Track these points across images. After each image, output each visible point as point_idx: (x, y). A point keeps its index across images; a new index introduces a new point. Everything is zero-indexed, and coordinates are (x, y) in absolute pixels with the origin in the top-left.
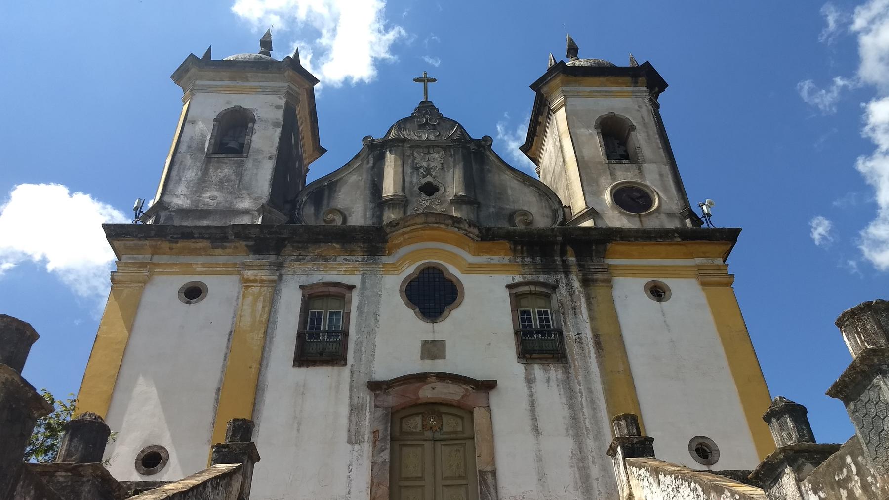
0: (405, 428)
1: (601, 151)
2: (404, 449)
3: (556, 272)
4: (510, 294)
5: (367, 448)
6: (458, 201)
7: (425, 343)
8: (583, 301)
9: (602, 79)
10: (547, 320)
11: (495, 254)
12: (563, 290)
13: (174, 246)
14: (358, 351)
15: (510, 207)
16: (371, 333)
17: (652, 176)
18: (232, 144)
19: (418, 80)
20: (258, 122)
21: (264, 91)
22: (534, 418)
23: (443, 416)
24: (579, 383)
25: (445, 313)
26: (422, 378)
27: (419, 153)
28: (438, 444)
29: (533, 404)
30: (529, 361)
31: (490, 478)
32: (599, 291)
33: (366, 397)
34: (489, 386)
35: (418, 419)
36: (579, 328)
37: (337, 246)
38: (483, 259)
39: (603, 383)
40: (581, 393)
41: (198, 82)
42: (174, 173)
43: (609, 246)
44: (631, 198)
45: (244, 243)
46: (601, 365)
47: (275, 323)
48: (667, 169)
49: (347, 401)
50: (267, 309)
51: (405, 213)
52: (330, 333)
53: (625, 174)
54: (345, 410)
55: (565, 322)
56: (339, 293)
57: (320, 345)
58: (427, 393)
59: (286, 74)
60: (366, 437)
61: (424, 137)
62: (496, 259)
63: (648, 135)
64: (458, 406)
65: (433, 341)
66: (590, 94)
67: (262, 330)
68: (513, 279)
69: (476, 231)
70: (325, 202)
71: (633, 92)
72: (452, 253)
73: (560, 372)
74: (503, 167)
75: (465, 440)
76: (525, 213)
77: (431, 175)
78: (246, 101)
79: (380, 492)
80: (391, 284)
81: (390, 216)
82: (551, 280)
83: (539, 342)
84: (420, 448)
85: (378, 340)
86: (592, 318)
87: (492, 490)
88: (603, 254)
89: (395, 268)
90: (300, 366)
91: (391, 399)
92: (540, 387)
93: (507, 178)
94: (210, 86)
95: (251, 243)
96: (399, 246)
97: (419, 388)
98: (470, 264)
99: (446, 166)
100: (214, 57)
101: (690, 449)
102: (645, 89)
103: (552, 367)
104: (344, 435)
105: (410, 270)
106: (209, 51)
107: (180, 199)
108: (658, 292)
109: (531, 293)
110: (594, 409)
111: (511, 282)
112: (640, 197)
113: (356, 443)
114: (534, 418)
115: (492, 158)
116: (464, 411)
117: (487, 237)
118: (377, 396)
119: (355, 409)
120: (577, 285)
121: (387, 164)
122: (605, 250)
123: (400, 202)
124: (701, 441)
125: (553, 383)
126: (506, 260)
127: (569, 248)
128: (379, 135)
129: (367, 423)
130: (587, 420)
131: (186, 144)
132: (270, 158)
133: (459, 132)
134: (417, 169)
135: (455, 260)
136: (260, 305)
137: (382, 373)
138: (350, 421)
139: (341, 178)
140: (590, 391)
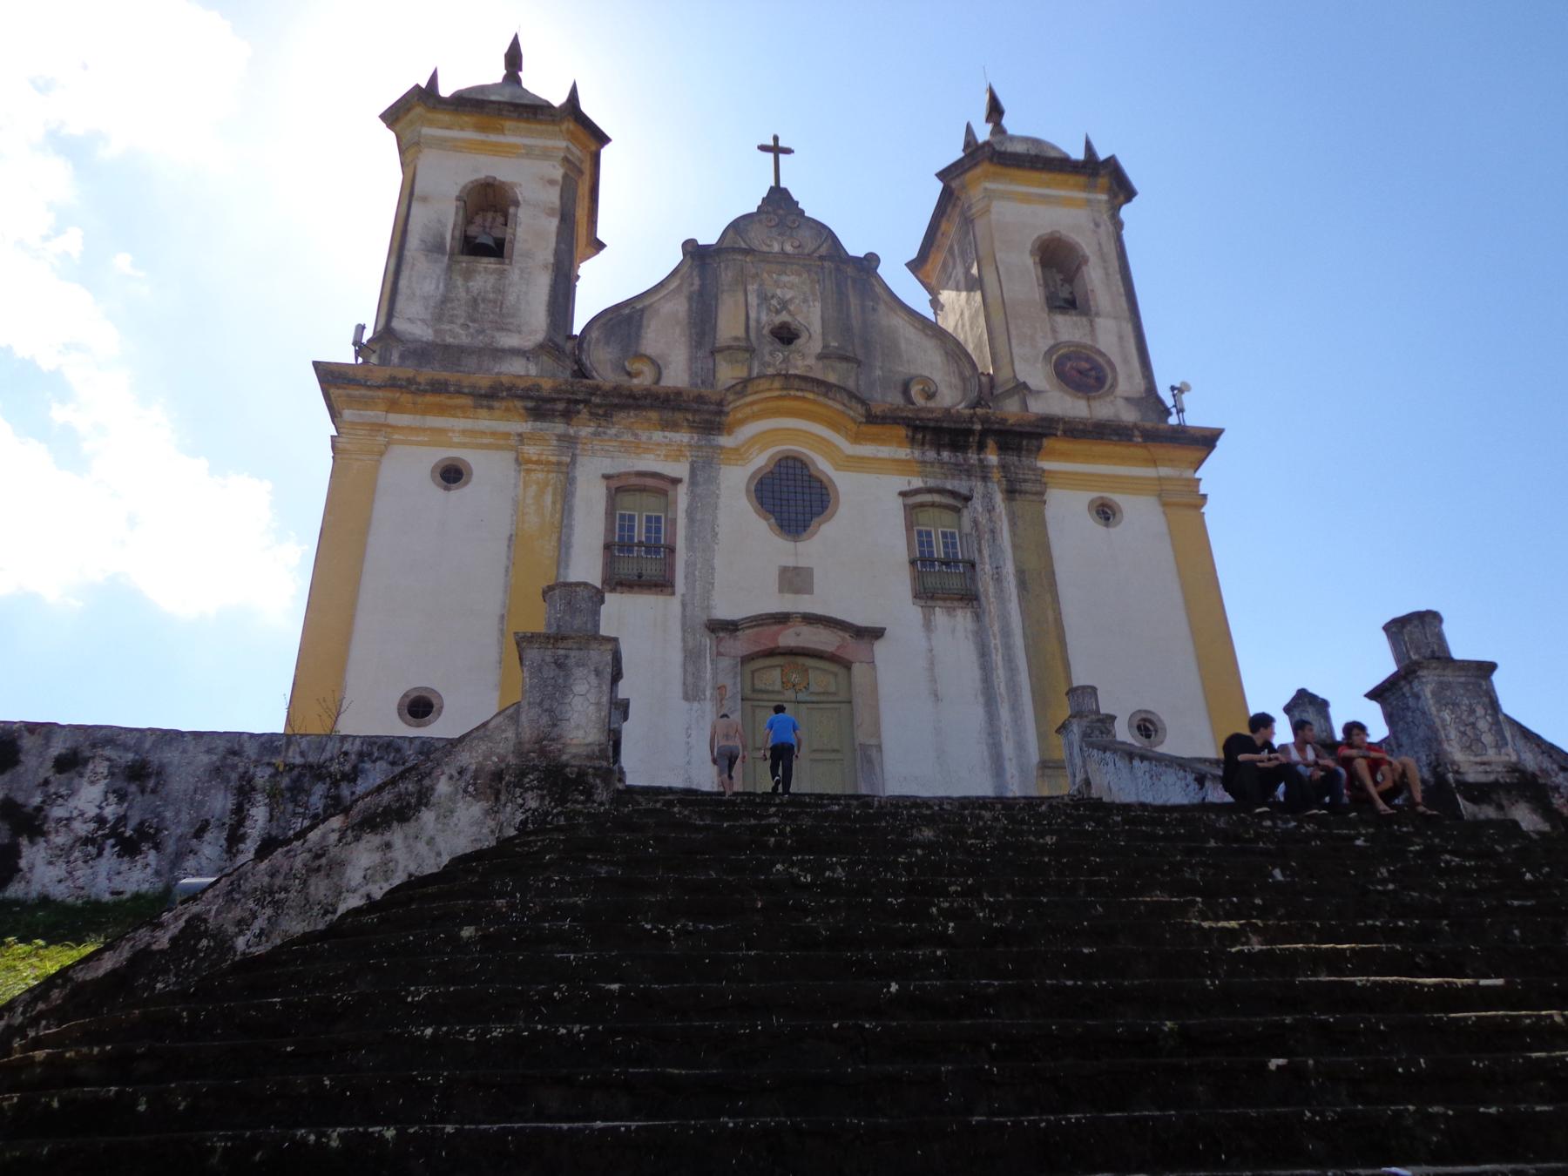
0: (759, 685)
1: (1037, 294)
7: (784, 571)
9: (1045, 176)
12: (977, 504)
13: (419, 400)
15: (904, 370)
17: (1107, 337)
19: (763, 148)
21: (529, 153)
22: (933, 680)
26: (782, 619)
27: (770, 273)
30: (930, 603)
31: (874, 753)
34: (877, 633)
35: (777, 673)
37: (654, 415)
38: (867, 450)
39: (1025, 636)
41: (426, 131)
42: (403, 283)
43: (1046, 442)
45: (519, 404)
46: (1025, 614)
48: (1128, 328)
49: (678, 644)
50: (558, 506)
53: (1069, 329)
54: (676, 657)
55: (980, 551)
56: (661, 486)
58: (788, 638)
59: (564, 127)
60: (708, 694)
61: (776, 248)
62: (885, 451)
63: (1107, 274)
64: (832, 658)
65: (795, 568)
66: (1027, 199)
67: (555, 537)
72: (824, 439)
76: (925, 380)
77: (789, 312)
78: (503, 170)
80: (734, 480)
82: (961, 485)
83: (944, 578)
85: (717, 562)
86: (1015, 547)
89: (738, 454)
91: (740, 645)
93: (898, 322)
94: (445, 140)
95: (530, 404)
96: (742, 422)
100: (445, 90)
102: (1104, 197)
104: (677, 689)
105: (760, 460)
106: (434, 79)
107: (415, 325)
108: (1105, 513)
109: (933, 505)
111: (906, 488)
115: (878, 289)
118: (719, 640)
119: (691, 656)
120: (999, 498)
122: (1039, 448)
123: (745, 349)
127: (991, 443)
129: (708, 676)
136: (548, 499)
137: (725, 610)
138: (685, 671)
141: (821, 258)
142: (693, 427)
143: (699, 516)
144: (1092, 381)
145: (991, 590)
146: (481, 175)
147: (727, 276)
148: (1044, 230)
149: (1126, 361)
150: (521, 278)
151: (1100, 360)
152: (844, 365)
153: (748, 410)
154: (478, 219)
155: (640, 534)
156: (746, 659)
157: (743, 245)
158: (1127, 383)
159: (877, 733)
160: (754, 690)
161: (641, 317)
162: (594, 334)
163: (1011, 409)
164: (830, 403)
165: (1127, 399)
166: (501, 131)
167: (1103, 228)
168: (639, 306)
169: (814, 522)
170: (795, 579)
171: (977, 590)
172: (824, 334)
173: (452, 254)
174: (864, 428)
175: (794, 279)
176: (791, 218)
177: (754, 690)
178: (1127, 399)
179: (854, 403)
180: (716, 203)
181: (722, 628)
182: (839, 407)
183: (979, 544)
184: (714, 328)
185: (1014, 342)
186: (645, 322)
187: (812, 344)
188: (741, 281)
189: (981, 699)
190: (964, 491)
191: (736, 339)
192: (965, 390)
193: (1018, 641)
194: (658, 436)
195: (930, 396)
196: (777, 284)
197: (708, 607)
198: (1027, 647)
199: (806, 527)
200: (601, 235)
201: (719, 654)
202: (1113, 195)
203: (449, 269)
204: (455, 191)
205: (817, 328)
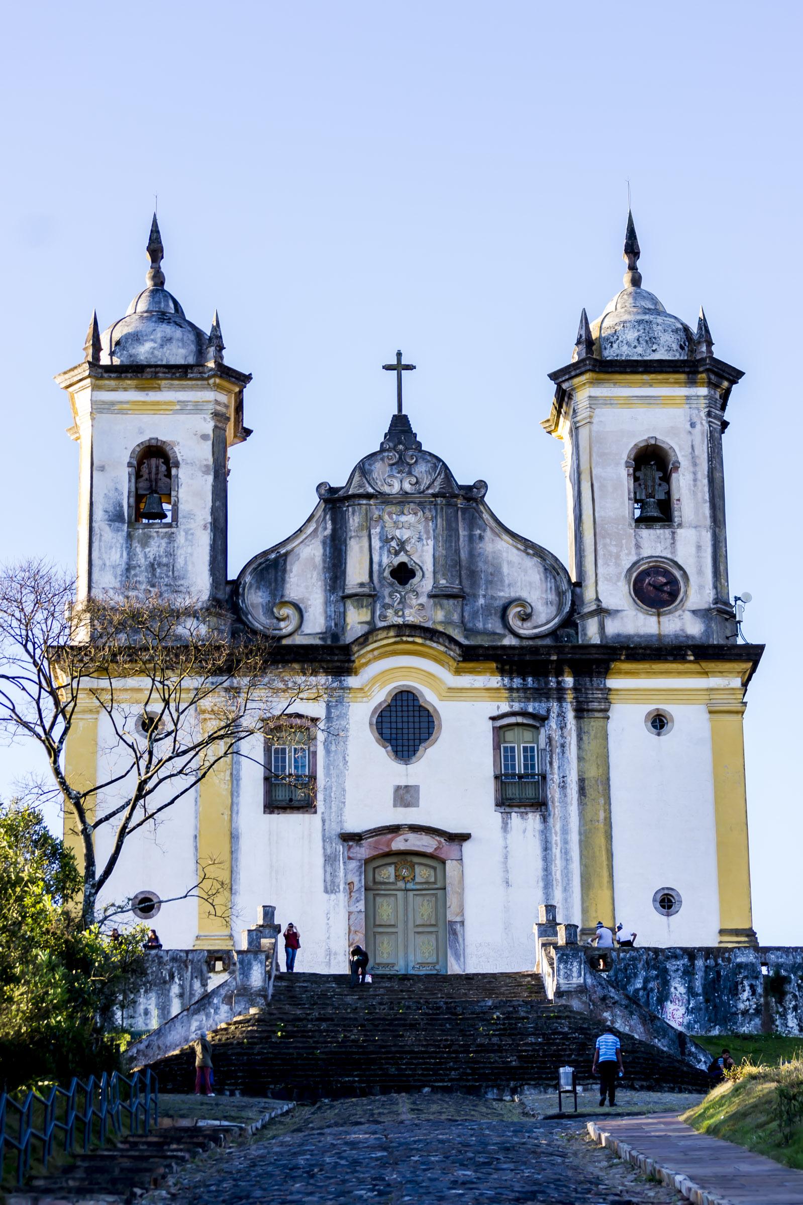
2: (379, 900)
3: (548, 699)
4: (494, 728)
5: (342, 897)
7: (398, 788)
10: (532, 757)
11: (479, 673)
12: (553, 723)
15: (505, 594)
16: (341, 775)
17: (687, 546)
19: (388, 368)
21: (183, 408)
23: (416, 866)
24: (556, 833)
25: (418, 754)
26: (395, 829)
27: (390, 514)
28: (411, 894)
30: (508, 810)
31: (458, 927)
32: (592, 725)
34: (462, 838)
35: (391, 870)
36: (565, 771)
37: (296, 666)
38: (466, 681)
39: (580, 834)
44: (657, 587)
46: (582, 814)
48: (707, 537)
49: (321, 851)
51: (373, 613)
53: (654, 543)
54: (320, 860)
55: (551, 763)
56: (304, 726)
58: (399, 844)
59: (211, 381)
60: (341, 888)
61: (396, 489)
63: (695, 480)
65: (406, 787)
66: (628, 402)
67: (228, 773)
68: (498, 707)
71: (688, 398)
74: (498, 529)
75: (438, 890)
80: (360, 714)
83: (520, 790)
84: (393, 899)
85: (348, 785)
86: (580, 759)
88: (605, 672)
90: (271, 812)
91: (363, 851)
94: (113, 403)
97: (392, 840)
98: (450, 689)
99: (424, 537)
101: (654, 900)
103: (530, 815)
104: (320, 886)
105: (380, 696)
108: (659, 722)
109: (518, 724)
111: (495, 713)
113: (332, 892)
115: (486, 516)
116: (436, 860)
117: (471, 656)
119: (330, 860)
120: (570, 715)
123: (368, 597)
124: (666, 892)
125: (530, 833)
127: (567, 669)
128: (339, 480)
131: (101, 507)
133: (442, 476)
138: (325, 871)
139: (292, 550)
140: (566, 842)
141: (435, 496)
142: (327, 672)
143: (333, 748)
144: (665, 596)
145: (557, 796)
146: (145, 438)
147: (354, 521)
149: (700, 572)
150: (186, 539)
151: (677, 574)
152: (451, 602)
153: (370, 656)
156: (367, 861)
157: (371, 490)
158: (698, 593)
159: (462, 912)
161: (285, 561)
162: (248, 579)
163: (592, 632)
164: (435, 645)
166: (159, 389)
167: (698, 426)
168: (283, 551)
169: (421, 748)
170: (405, 796)
172: (435, 573)
173: (130, 523)
174: (462, 665)
176: (410, 453)
177: (375, 882)
179: (453, 647)
180: (342, 446)
181: (351, 838)
182: (442, 648)
183: (551, 757)
184: (344, 573)
185: (600, 562)
186: (288, 568)
187: (425, 583)
188: (367, 525)
189: (541, 884)
190: (543, 712)
191: (362, 585)
194: (300, 679)
195: (526, 617)
196: (396, 525)
198: (580, 841)
199: (415, 752)
201: (350, 858)
203: (129, 537)
205: (429, 567)
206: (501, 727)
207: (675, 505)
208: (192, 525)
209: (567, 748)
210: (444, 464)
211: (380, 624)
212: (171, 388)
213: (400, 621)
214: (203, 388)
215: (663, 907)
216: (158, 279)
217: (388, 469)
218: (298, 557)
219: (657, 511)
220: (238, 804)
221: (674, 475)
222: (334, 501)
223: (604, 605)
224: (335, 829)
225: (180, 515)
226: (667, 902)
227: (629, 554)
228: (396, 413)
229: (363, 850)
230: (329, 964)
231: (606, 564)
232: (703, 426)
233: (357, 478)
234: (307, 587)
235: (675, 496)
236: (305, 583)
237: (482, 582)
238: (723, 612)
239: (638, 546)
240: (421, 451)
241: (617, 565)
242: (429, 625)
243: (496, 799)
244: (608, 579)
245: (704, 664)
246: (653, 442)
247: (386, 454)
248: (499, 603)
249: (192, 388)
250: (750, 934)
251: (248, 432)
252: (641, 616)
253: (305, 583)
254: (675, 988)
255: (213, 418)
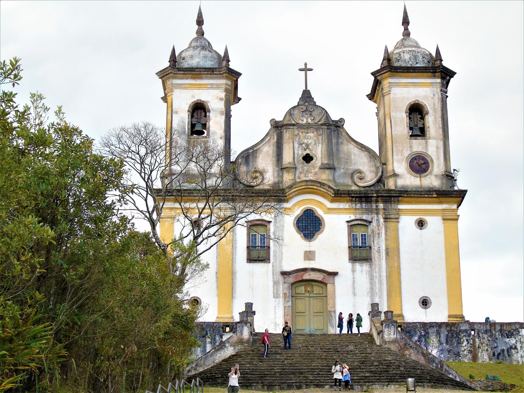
0: (297, 292)
2: (298, 301)
5: (281, 300)
6: (324, 167)
7: (306, 252)
8: (383, 229)
10: (365, 239)
11: (341, 202)
12: (374, 223)
14: (275, 256)
15: (353, 167)
17: (432, 147)
18: (198, 128)
19: (301, 70)
20: (211, 111)
21: (212, 87)
22: (354, 289)
24: (376, 272)
25: (315, 237)
26: (305, 270)
27: (302, 133)
28: (312, 299)
29: (354, 282)
32: (391, 225)
33: (281, 278)
34: (335, 274)
35: (303, 288)
36: (379, 245)
38: (335, 205)
39: (387, 272)
40: (376, 277)
43: (400, 198)
44: (419, 165)
46: (387, 263)
47: (236, 240)
48: (441, 144)
49: (272, 279)
51: (295, 175)
52: (261, 247)
53: (418, 146)
54: (271, 284)
55: (373, 241)
56: (264, 224)
57: (258, 253)
58: (306, 276)
59: (224, 75)
60: (281, 296)
62: (342, 205)
63: (435, 118)
66: (406, 85)
67: (231, 245)
68: (350, 217)
69: (332, 191)
70: (251, 164)
71: (432, 83)
73: (368, 266)
74: (350, 140)
76: (360, 172)
77: (309, 149)
79: (288, 318)
81: (288, 178)
83: (360, 252)
84: (304, 300)
86: (386, 239)
87: (334, 318)
90: (250, 262)
91: (291, 279)
92: (358, 274)
94: (181, 84)
97: (303, 274)
98: (329, 209)
99: (317, 142)
101: (419, 302)
102: (439, 80)
104: (272, 295)
105: (298, 211)
108: (421, 224)
109: (358, 224)
110: (381, 284)
111: (349, 219)
112: (424, 164)
114: (354, 289)
115: (344, 134)
118: (285, 278)
119: (276, 283)
120: (382, 220)
121: (284, 141)
125: (364, 272)
126: (347, 205)
128: (280, 118)
129: (281, 289)
130: (377, 290)
132: (221, 138)
133: (325, 116)
134: (301, 144)
135: (321, 206)
138: (274, 288)
140: (380, 276)
141: (322, 125)
146: (195, 99)
147: (287, 135)
148: (411, 100)
149: (438, 159)
153: (294, 194)
154: (195, 115)
155: (258, 243)
156: (293, 284)
157: (294, 122)
158: (437, 167)
160: (296, 294)
161: (256, 153)
163: (391, 184)
164: (322, 189)
165: (436, 176)
166: (201, 78)
170: (309, 255)
171: (371, 256)
172: (322, 158)
173: (188, 136)
174: (335, 198)
175: (311, 135)
178: (436, 176)
179: (330, 190)
182: (325, 191)
183: (373, 239)
184: (282, 158)
185: (394, 154)
190: (370, 220)
191: (290, 163)
192: (377, 173)
193: (384, 274)
197: (281, 267)
200: (239, 95)
202: (443, 78)
204: (187, 109)
205: (319, 155)
206: (351, 226)
207: (426, 129)
208: (216, 137)
209: (380, 235)
210: (326, 111)
211: (298, 180)
212: (207, 78)
213: (307, 179)
214: (220, 78)
215: (423, 305)
216: (201, 33)
217: (301, 113)
218: (262, 151)
219: (419, 131)
220: (235, 258)
221: (426, 117)
222: (278, 127)
223: (396, 172)
224: (279, 270)
225: (210, 133)
226: (425, 303)
227: (407, 150)
228: (304, 89)
229: (291, 279)
230: (276, 329)
231: (397, 155)
232: (438, 95)
233: (287, 117)
234: (266, 164)
235: (427, 125)
236: (265, 162)
237: (343, 162)
238: (449, 177)
239: (411, 147)
240: (315, 105)
241: (402, 155)
242: (319, 180)
243: (349, 257)
244: (398, 161)
245: (440, 199)
246: (417, 102)
247: (300, 107)
248: (350, 171)
249: (216, 78)
250: (463, 317)
251: (240, 99)
252: (413, 177)
253: (265, 162)
254: (433, 341)
255: (225, 91)
